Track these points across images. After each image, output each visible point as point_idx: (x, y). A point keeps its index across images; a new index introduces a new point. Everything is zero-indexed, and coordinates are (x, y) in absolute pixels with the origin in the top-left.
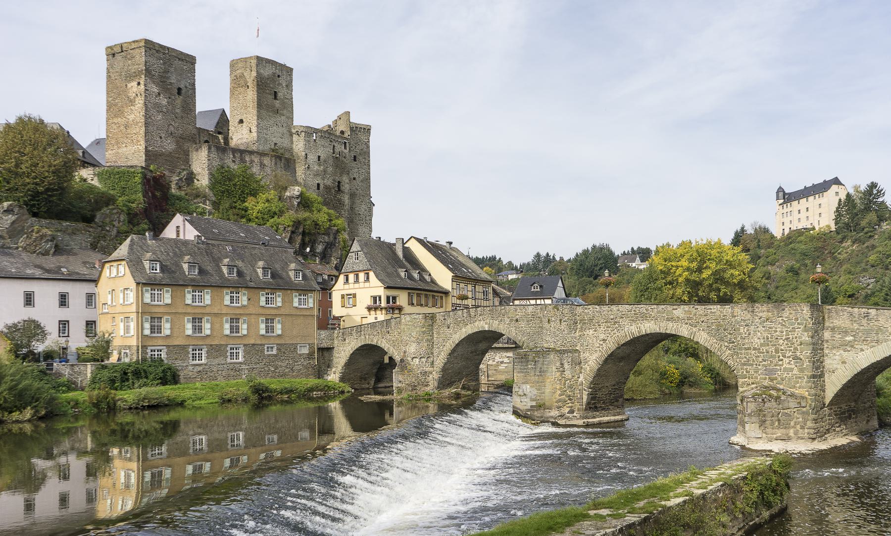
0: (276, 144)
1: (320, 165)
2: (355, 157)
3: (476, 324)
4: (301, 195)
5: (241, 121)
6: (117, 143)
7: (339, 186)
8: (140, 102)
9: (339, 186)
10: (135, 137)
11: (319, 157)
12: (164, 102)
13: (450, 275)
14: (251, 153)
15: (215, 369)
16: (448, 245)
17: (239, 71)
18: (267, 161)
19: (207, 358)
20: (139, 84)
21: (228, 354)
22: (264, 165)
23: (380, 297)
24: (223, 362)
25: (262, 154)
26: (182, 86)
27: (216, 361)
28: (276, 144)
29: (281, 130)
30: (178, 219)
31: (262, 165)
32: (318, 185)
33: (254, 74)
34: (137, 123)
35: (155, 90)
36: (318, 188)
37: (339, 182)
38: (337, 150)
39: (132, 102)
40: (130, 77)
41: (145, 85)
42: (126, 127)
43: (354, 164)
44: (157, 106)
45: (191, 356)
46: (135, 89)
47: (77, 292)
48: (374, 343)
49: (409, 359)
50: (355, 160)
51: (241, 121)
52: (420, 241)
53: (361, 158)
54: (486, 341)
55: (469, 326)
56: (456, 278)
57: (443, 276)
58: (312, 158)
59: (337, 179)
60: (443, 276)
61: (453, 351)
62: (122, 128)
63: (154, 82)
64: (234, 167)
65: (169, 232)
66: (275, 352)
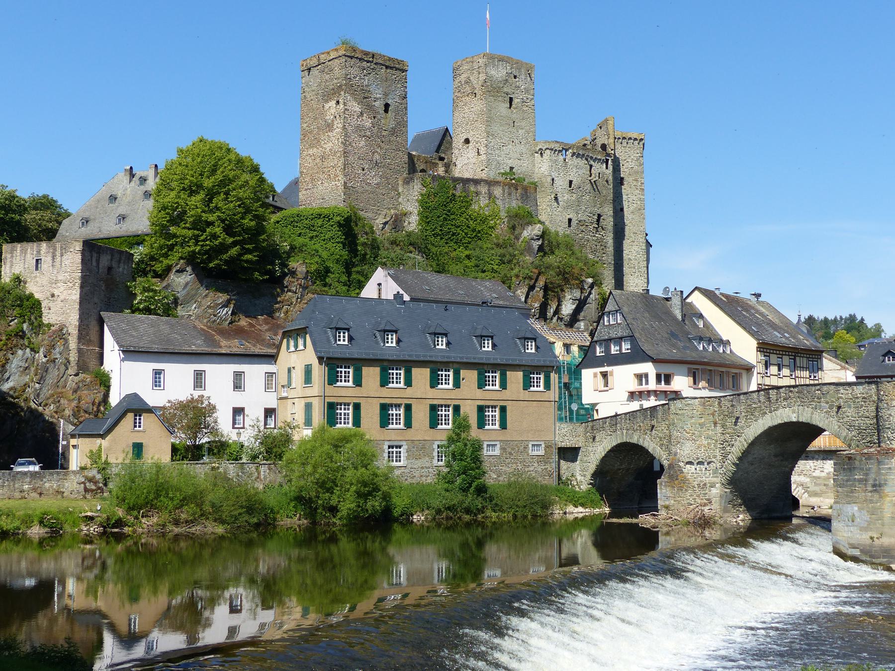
0: (512, 168)
1: (571, 192)
3: (778, 413)
4: (543, 236)
5: (467, 141)
6: (313, 180)
7: (598, 220)
8: (338, 125)
9: (598, 220)
10: (332, 171)
11: (571, 182)
12: (368, 123)
13: (753, 343)
14: (476, 182)
15: (417, 474)
16: (754, 299)
17: (463, 76)
18: (498, 191)
19: (408, 458)
20: (338, 102)
21: (435, 454)
22: (495, 197)
23: (646, 375)
24: (428, 465)
25: (490, 183)
27: (418, 463)
28: (512, 168)
30: (379, 275)
31: (490, 195)
32: (570, 220)
33: (482, 77)
34: (336, 153)
35: (356, 108)
36: (570, 226)
37: (599, 216)
39: (330, 127)
40: (330, 94)
41: (345, 104)
42: (323, 158)
44: (359, 128)
45: (386, 455)
46: (333, 111)
47: (255, 372)
48: (634, 440)
49: (682, 464)
51: (467, 141)
52: (709, 294)
53: (631, 179)
54: (794, 440)
55: (768, 416)
56: (764, 348)
57: (743, 346)
58: (561, 184)
60: (743, 346)
61: (745, 454)
62: (318, 160)
65: (369, 291)
66: (497, 452)
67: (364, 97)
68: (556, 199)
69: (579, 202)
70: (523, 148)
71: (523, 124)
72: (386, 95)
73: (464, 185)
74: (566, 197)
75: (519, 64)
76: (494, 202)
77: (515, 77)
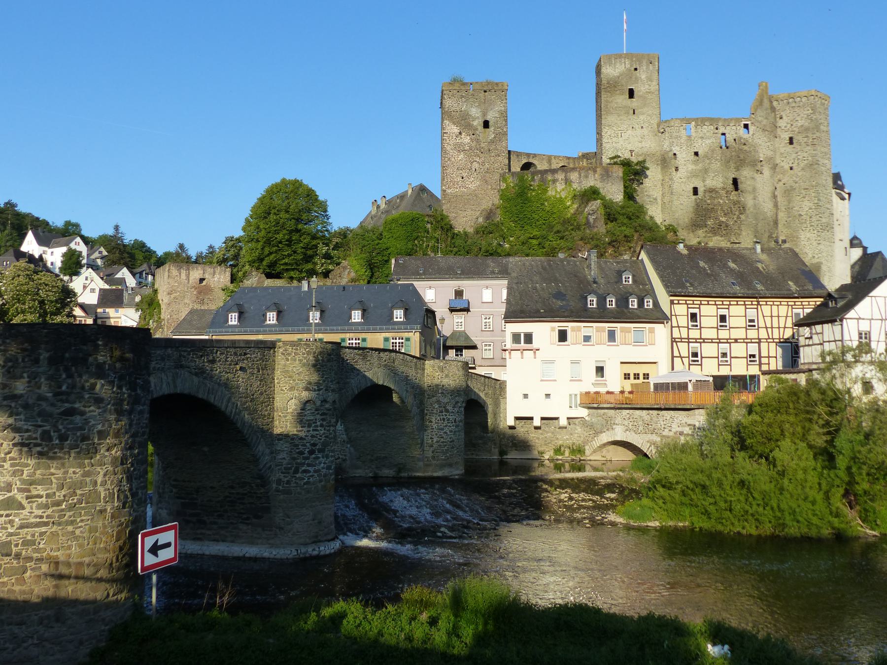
0: (631, 151)
1: (695, 163)
11: (696, 154)
12: (466, 139)
29: (639, 132)
31: (567, 181)
32: (695, 191)
35: (455, 130)
37: (735, 182)
38: (730, 137)
63: (454, 123)
67: (464, 122)
70: (645, 131)
71: (645, 110)
72: (484, 114)
73: (542, 176)
74: (691, 167)
75: (639, 58)
76: (570, 185)
77: (636, 69)
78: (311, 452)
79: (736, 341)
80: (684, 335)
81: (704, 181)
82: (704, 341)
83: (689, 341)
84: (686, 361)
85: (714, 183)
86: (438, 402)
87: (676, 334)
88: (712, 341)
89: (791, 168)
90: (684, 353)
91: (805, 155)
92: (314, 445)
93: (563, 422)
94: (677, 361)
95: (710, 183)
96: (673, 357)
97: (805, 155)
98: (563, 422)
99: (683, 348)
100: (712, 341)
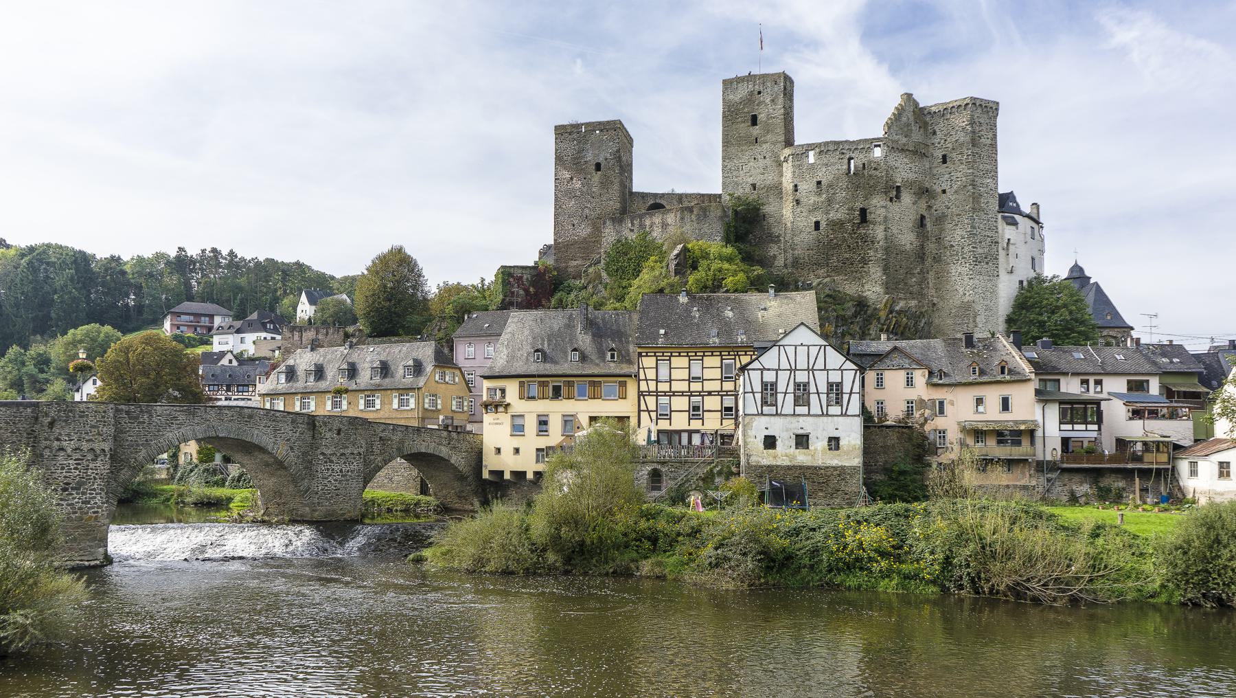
0: (754, 186)
2: (944, 157)
12: (577, 184)
26: (601, 160)
29: (761, 163)
31: (665, 225)
32: (817, 225)
37: (863, 212)
43: (942, 169)
50: (944, 161)
58: (806, 187)
59: (859, 205)
64: (632, 236)
68: (798, 202)
69: (830, 201)
74: (813, 199)
77: (759, 93)
78: (64, 490)
79: (710, 393)
80: (653, 388)
81: (827, 213)
82: (674, 394)
83: (657, 394)
84: (653, 415)
85: (839, 216)
86: (323, 454)
87: (643, 387)
88: (682, 394)
89: (944, 192)
90: (652, 406)
91: (959, 174)
92: (68, 484)
93: (530, 476)
94: (644, 415)
95: (832, 215)
96: (640, 411)
97: (959, 174)
98: (530, 476)
99: (651, 401)
100: (682, 394)
